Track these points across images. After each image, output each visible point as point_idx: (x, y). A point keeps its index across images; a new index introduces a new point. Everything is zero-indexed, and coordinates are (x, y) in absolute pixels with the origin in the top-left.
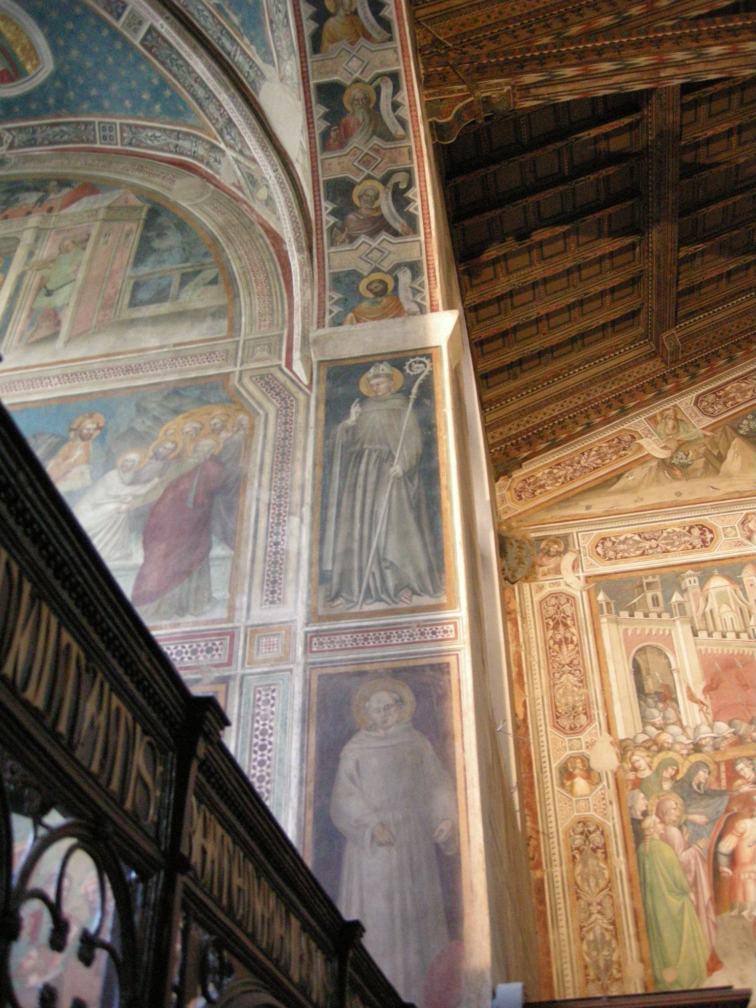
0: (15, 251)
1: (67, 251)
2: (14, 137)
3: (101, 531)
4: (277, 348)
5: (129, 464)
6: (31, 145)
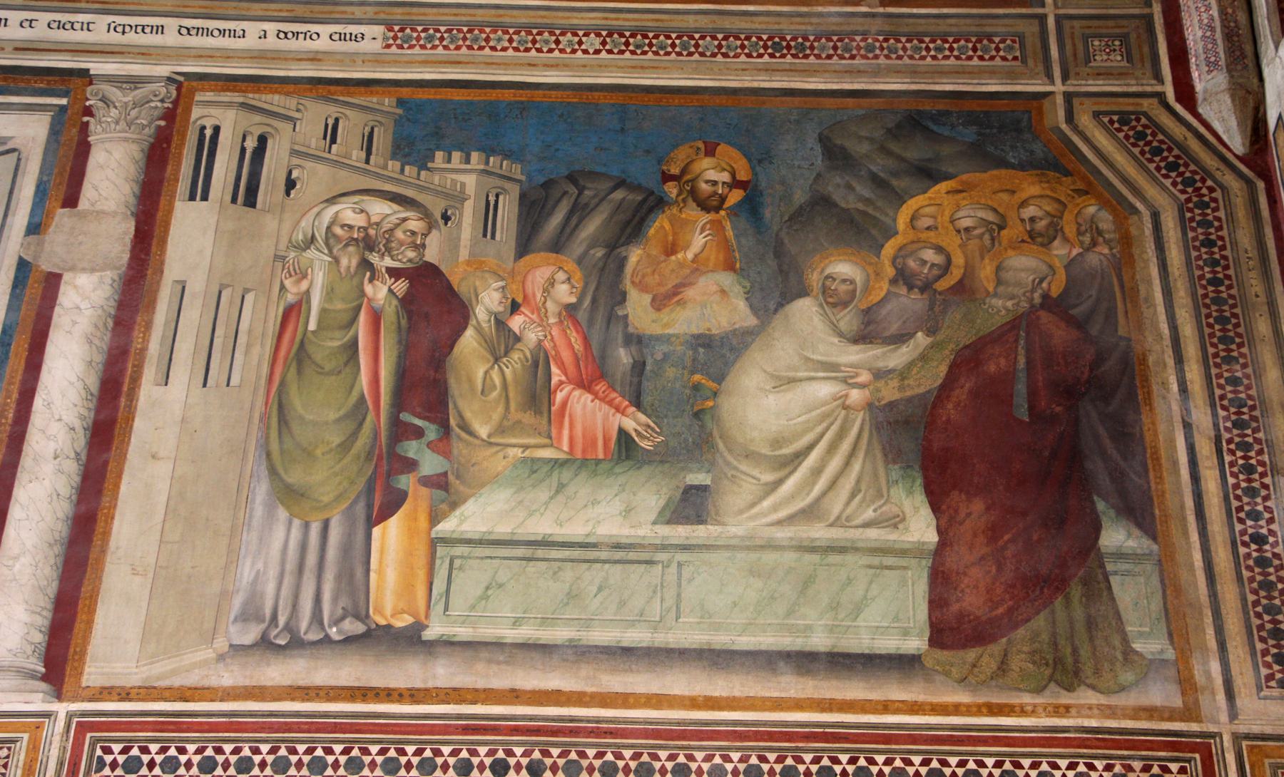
3: (811, 447)
4: (1146, 50)
5: (843, 288)
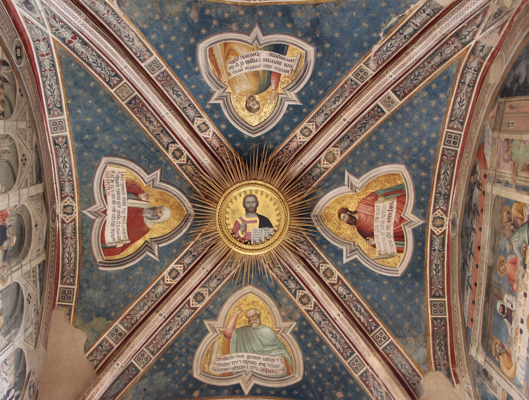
0: (502, 198)
1: (512, 153)
2: (440, 208)
6: (448, 199)
